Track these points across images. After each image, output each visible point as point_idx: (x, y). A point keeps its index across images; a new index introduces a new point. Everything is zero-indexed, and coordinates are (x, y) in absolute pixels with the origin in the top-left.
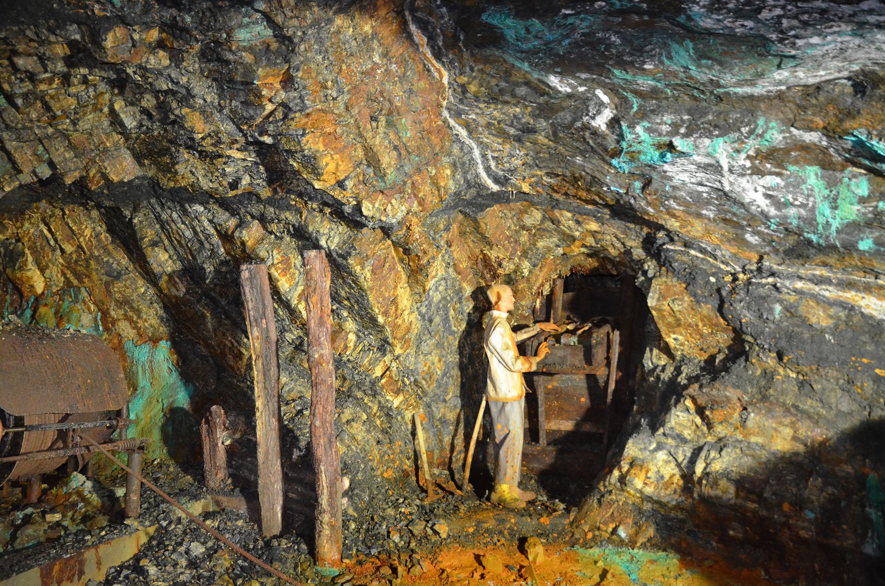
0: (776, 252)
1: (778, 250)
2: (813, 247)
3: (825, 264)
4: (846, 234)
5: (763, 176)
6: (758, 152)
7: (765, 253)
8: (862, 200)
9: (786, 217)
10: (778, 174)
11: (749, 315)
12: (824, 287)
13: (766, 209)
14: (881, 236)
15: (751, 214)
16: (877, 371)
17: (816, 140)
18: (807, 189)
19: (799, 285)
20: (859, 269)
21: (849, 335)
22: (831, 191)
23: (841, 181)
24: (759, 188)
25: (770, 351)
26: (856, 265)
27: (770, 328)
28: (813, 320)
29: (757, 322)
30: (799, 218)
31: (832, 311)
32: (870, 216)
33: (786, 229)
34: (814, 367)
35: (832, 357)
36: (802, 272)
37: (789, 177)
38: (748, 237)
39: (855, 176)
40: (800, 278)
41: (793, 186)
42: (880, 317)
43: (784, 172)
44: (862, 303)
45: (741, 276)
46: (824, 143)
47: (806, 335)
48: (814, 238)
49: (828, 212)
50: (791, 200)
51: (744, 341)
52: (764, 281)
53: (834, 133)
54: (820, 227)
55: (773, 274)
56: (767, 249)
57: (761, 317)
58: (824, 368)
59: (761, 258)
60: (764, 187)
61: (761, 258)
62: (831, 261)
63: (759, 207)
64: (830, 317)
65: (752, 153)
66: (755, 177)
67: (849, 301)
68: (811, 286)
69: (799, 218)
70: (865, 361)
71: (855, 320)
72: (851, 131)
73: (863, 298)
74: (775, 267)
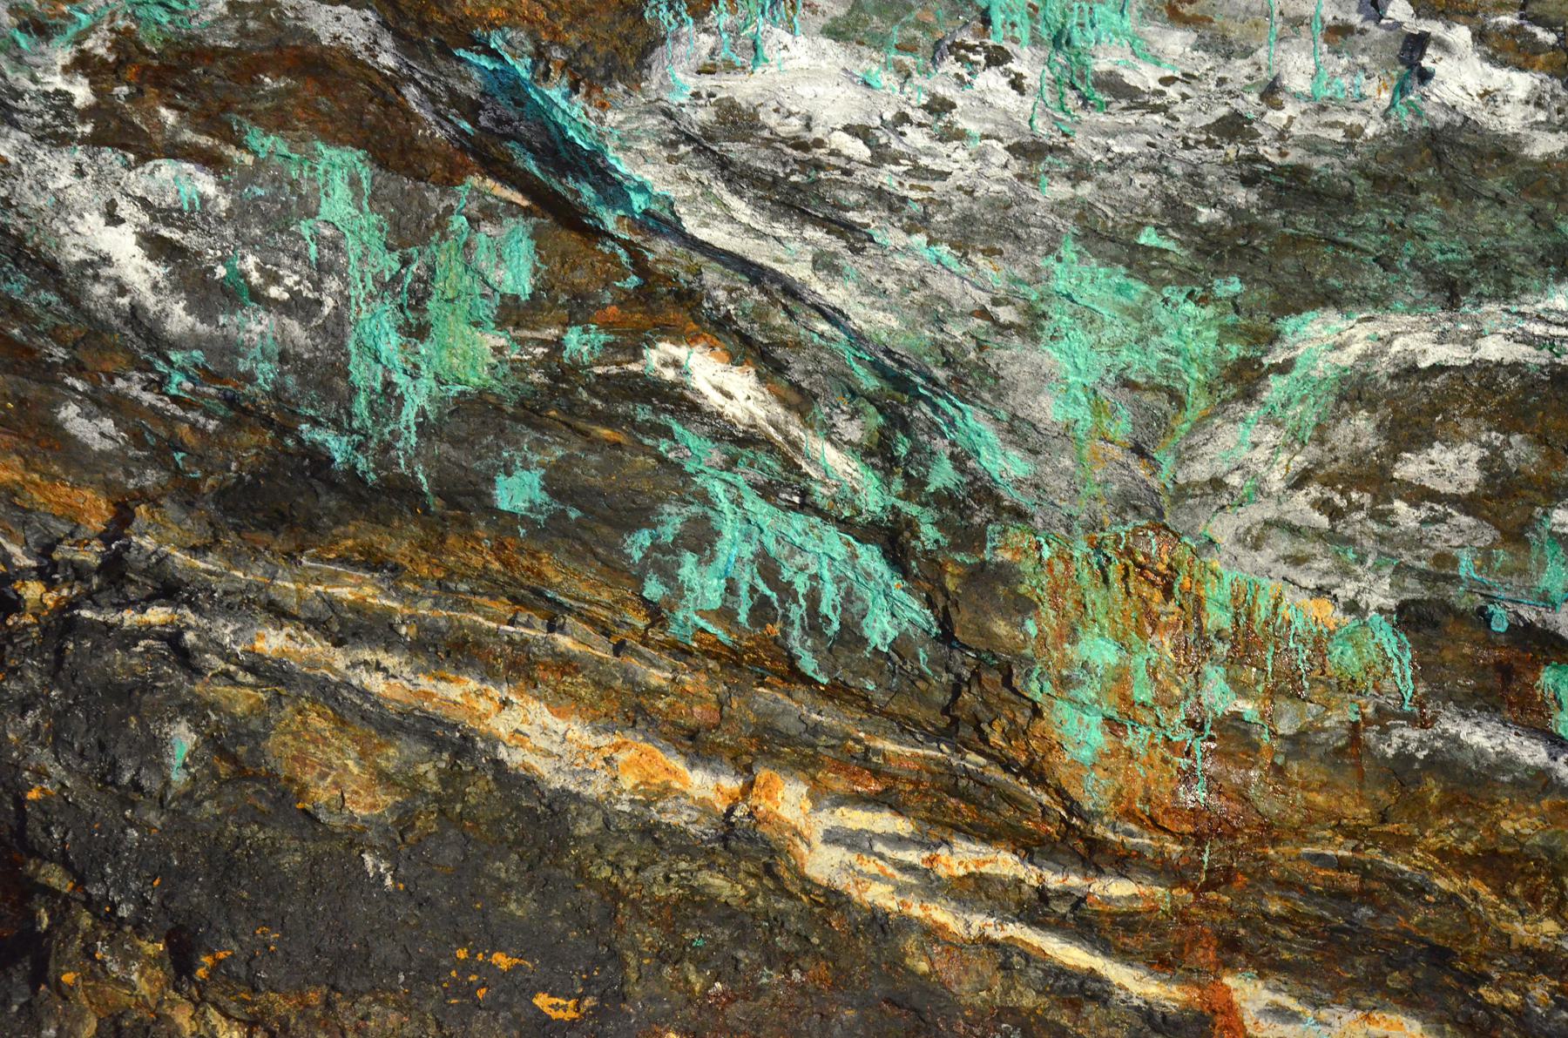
0: (187, 494)
1: (194, 485)
2: (333, 486)
3: (373, 562)
4: (455, 442)
5: (144, 158)
6: (124, 43)
7: (142, 495)
8: (512, 313)
9: (230, 349)
10: (211, 161)
11: (56, 770)
12: (366, 655)
13: (150, 301)
14: (567, 459)
15: (89, 316)
16: (542, 1001)
17: (358, 42)
18: (319, 239)
19: (272, 641)
20: (495, 588)
21: (451, 855)
22: (406, 262)
23: (441, 223)
24: (125, 209)
25: (139, 929)
26: (485, 573)
27: (144, 827)
28: (322, 794)
29: (90, 800)
30: (283, 357)
31: (392, 756)
32: (536, 377)
33: (231, 401)
34: (314, 997)
35: (385, 950)
36: (286, 586)
37: (249, 177)
38: (70, 415)
39: (489, 213)
40: (278, 613)
41: (266, 220)
42: (557, 783)
43: (231, 151)
44: (501, 725)
45: (33, 591)
46: (387, 60)
47: (291, 861)
48: (337, 446)
49: (390, 344)
50: (255, 278)
51: (34, 889)
52: (130, 618)
53: (423, 26)
54: (361, 405)
55: (169, 590)
56: (151, 477)
57: (108, 776)
58: (354, 996)
59: (123, 517)
60: (144, 204)
61: (123, 517)
62: (398, 547)
63: (122, 290)
64: (384, 778)
65: (98, 45)
66: (107, 154)
67: (457, 715)
68: (319, 648)
69: (283, 357)
70: (502, 961)
71: (473, 793)
72: (478, 31)
73: (505, 703)
74: (180, 557)
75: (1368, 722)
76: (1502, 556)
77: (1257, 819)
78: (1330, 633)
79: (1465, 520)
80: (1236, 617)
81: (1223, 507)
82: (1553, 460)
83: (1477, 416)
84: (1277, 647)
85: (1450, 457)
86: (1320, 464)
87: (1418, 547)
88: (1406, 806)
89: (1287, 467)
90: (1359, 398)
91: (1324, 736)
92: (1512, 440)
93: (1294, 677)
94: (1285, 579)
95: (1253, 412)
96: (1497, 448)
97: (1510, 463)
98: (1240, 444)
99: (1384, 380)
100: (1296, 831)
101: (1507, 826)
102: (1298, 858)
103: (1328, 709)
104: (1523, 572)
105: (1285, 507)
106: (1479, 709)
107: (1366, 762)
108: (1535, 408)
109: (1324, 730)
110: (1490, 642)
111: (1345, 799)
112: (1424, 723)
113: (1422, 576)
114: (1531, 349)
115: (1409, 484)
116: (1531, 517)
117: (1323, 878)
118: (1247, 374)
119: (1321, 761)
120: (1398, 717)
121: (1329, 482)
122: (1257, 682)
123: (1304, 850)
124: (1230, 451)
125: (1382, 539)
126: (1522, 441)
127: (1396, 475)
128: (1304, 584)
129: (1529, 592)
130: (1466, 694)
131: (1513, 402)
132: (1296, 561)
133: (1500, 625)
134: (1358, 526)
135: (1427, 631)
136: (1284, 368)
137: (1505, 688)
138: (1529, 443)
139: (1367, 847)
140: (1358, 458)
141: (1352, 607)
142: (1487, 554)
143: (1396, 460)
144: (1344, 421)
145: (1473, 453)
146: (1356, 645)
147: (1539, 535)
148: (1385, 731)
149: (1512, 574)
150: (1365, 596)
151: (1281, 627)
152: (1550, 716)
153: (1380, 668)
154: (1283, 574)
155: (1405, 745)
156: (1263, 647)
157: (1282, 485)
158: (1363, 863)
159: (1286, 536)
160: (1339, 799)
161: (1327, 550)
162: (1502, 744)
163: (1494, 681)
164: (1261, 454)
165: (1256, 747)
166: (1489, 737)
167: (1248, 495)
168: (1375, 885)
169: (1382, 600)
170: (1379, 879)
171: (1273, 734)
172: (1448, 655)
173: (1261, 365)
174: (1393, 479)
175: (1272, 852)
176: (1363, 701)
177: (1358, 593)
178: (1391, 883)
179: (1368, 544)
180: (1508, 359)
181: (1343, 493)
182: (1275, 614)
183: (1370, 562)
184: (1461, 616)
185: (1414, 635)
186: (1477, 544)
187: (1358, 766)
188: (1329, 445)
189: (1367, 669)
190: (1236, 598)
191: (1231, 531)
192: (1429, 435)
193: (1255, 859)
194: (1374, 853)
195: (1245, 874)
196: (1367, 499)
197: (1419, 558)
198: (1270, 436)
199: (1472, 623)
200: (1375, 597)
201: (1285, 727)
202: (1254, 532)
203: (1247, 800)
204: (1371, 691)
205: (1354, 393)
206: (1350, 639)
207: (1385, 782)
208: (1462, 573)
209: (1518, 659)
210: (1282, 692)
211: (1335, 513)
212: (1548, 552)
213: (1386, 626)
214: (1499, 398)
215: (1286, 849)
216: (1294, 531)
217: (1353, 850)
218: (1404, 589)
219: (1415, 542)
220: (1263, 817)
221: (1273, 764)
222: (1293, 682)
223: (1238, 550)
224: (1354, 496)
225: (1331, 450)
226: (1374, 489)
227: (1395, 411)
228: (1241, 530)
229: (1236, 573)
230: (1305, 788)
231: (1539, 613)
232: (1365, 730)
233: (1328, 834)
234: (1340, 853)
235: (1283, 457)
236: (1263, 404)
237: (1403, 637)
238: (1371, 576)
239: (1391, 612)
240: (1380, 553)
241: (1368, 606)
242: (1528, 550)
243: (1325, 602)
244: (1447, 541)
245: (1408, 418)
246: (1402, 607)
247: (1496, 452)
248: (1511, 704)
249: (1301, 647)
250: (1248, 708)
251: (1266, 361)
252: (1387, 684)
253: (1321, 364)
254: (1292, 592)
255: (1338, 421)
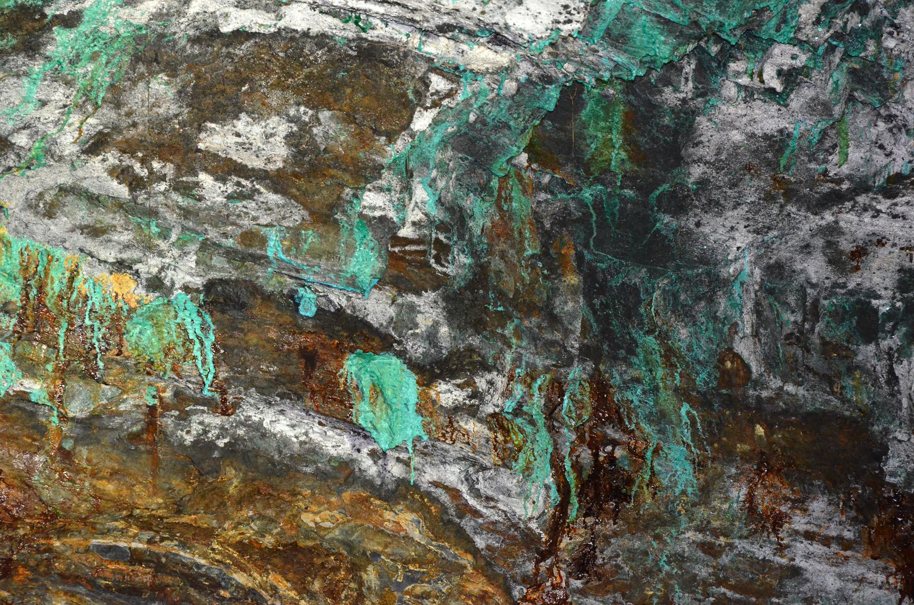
75: (166, 407)
76: (311, 237)
77: (39, 509)
78: (131, 310)
79: (274, 198)
80: (26, 287)
81: (9, 169)
82: (362, 141)
83: (285, 88)
84: (71, 324)
85: (257, 130)
86: (116, 129)
87: (225, 224)
88: (203, 497)
89: (80, 129)
90: (156, 60)
91: (118, 420)
92: (321, 116)
93: (88, 357)
94: (81, 250)
95: (37, 67)
96: (306, 124)
97: (319, 140)
98: (26, 101)
99: (183, 42)
100: (84, 521)
101: (307, 519)
102: (87, 550)
103: (124, 392)
104: (331, 255)
105: (80, 173)
106: (282, 396)
107: (161, 450)
108: (343, 83)
109: (120, 414)
110: (296, 327)
111: (137, 488)
112: (225, 410)
113: (230, 254)
114: (336, 21)
115: (215, 156)
116: (339, 198)
117: (114, 572)
118: (28, 25)
119: (113, 445)
120: (197, 402)
121: (128, 149)
122: (47, 360)
123: (94, 542)
124: (15, 108)
125: (186, 213)
126: (331, 118)
127: (201, 146)
128: (102, 257)
129: (338, 276)
130: (270, 380)
131: (321, 76)
132: (94, 232)
133: (308, 310)
134: (161, 198)
135: (234, 313)
136: (71, 21)
137: (308, 375)
138: (338, 119)
139: (162, 539)
140: (160, 124)
141: (155, 284)
142: (295, 236)
143: (200, 129)
144: (141, 85)
145: (283, 128)
146: (156, 325)
147: (348, 216)
148: (184, 417)
149: (320, 257)
150: (170, 273)
151: (77, 302)
152: (351, 406)
153: (180, 350)
154: (79, 245)
155: (205, 432)
156: (55, 322)
157: (75, 149)
158: (158, 556)
159: (83, 204)
160: (131, 487)
161: (128, 222)
162: (306, 434)
163: (297, 368)
164: (50, 113)
165: (42, 430)
166: (293, 426)
167: (37, 158)
168: (169, 580)
169: (188, 278)
170: (172, 573)
171: (63, 417)
172: (253, 339)
173: (44, 16)
174: (199, 151)
175: (57, 544)
176: (161, 384)
177: (162, 269)
178: (184, 576)
179: (172, 217)
180: (314, 31)
181: (144, 162)
182: (70, 288)
183: (173, 237)
184: (268, 298)
185: (218, 315)
186: (286, 223)
187: (152, 453)
188: (126, 109)
189: (167, 351)
190: (26, 269)
191: (21, 196)
192: (235, 105)
193: (38, 551)
194: (170, 546)
195: (25, 566)
196: (169, 170)
197: (225, 235)
198: (59, 95)
199: (279, 306)
200: (181, 275)
201: (75, 409)
202: (48, 198)
203: (30, 487)
204: (170, 374)
205: (150, 54)
206: (151, 318)
207: (183, 471)
208: (270, 253)
209: (323, 346)
210: (74, 372)
211: (135, 184)
212: (358, 235)
213: (192, 306)
214: (306, 70)
215: (74, 540)
216: (93, 200)
217: (150, 542)
218: (211, 268)
219: (220, 219)
220: (47, 506)
221: (61, 449)
222: (87, 361)
223: (28, 216)
224: (156, 165)
225: (129, 114)
226: (177, 159)
227: (198, 77)
228: (32, 195)
229: (26, 241)
230: (94, 475)
231: (349, 298)
232: (162, 415)
233: (120, 524)
234: (134, 545)
235: (75, 119)
236: (48, 59)
237: (208, 318)
238: (176, 252)
239: (197, 291)
240: (184, 228)
241: (173, 284)
242: (337, 234)
243: (127, 277)
244: (255, 219)
245: (212, 86)
246: (210, 286)
247: (305, 128)
248: (313, 392)
249: (97, 324)
250: (36, 389)
251: (49, 11)
252: (187, 366)
253: (111, 20)
254: (90, 265)
255: (134, 83)
